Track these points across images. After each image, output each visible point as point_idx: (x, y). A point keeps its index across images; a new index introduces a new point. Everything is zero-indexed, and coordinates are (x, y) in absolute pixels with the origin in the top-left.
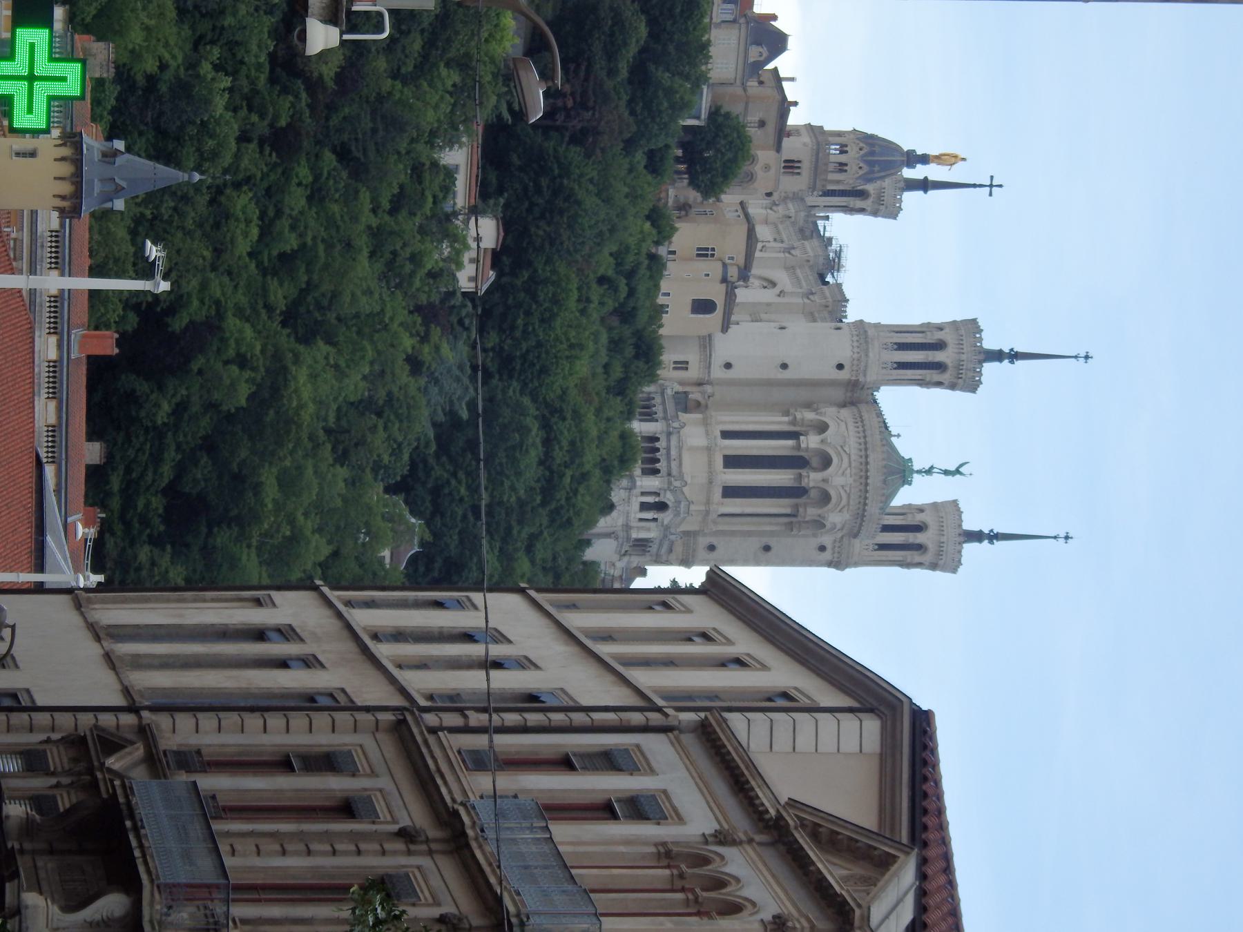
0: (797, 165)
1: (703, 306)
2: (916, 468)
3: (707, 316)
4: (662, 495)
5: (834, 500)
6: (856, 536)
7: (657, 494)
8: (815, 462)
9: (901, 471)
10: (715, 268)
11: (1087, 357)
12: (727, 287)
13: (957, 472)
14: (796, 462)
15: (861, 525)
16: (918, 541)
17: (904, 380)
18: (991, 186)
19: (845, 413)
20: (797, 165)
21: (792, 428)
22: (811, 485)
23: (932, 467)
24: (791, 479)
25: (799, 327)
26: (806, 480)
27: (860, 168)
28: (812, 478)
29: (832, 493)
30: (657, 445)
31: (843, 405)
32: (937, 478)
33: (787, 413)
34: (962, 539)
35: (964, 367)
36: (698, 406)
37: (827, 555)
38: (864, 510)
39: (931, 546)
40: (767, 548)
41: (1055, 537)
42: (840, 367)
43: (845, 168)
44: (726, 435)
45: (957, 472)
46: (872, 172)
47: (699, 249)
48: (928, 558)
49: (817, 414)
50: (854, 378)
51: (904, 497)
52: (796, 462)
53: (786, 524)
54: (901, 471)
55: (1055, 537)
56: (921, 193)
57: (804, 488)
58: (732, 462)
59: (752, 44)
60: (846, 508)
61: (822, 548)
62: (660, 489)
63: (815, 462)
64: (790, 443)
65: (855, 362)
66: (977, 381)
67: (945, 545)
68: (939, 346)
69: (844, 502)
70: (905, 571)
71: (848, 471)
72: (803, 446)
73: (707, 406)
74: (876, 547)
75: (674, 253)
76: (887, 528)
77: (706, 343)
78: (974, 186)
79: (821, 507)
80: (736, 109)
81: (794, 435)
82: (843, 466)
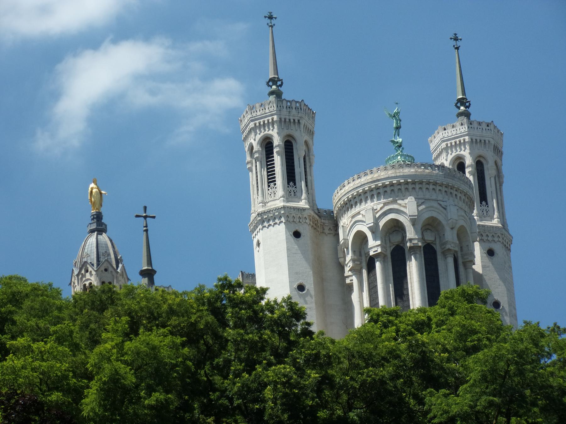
5: (435, 214)
26: (416, 242)
27: (106, 270)
29: (426, 216)
35: (287, 117)
37: (497, 248)
41: (457, 48)
42: (297, 235)
50: (308, 221)
55: (457, 48)
60: (441, 203)
63: (396, 239)
64: (378, 265)
66: (300, 105)
67: (474, 138)
68: (267, 144)
69: (435, 204)
70: (505, 180)
74: (484, 203)
79: (443, 227)
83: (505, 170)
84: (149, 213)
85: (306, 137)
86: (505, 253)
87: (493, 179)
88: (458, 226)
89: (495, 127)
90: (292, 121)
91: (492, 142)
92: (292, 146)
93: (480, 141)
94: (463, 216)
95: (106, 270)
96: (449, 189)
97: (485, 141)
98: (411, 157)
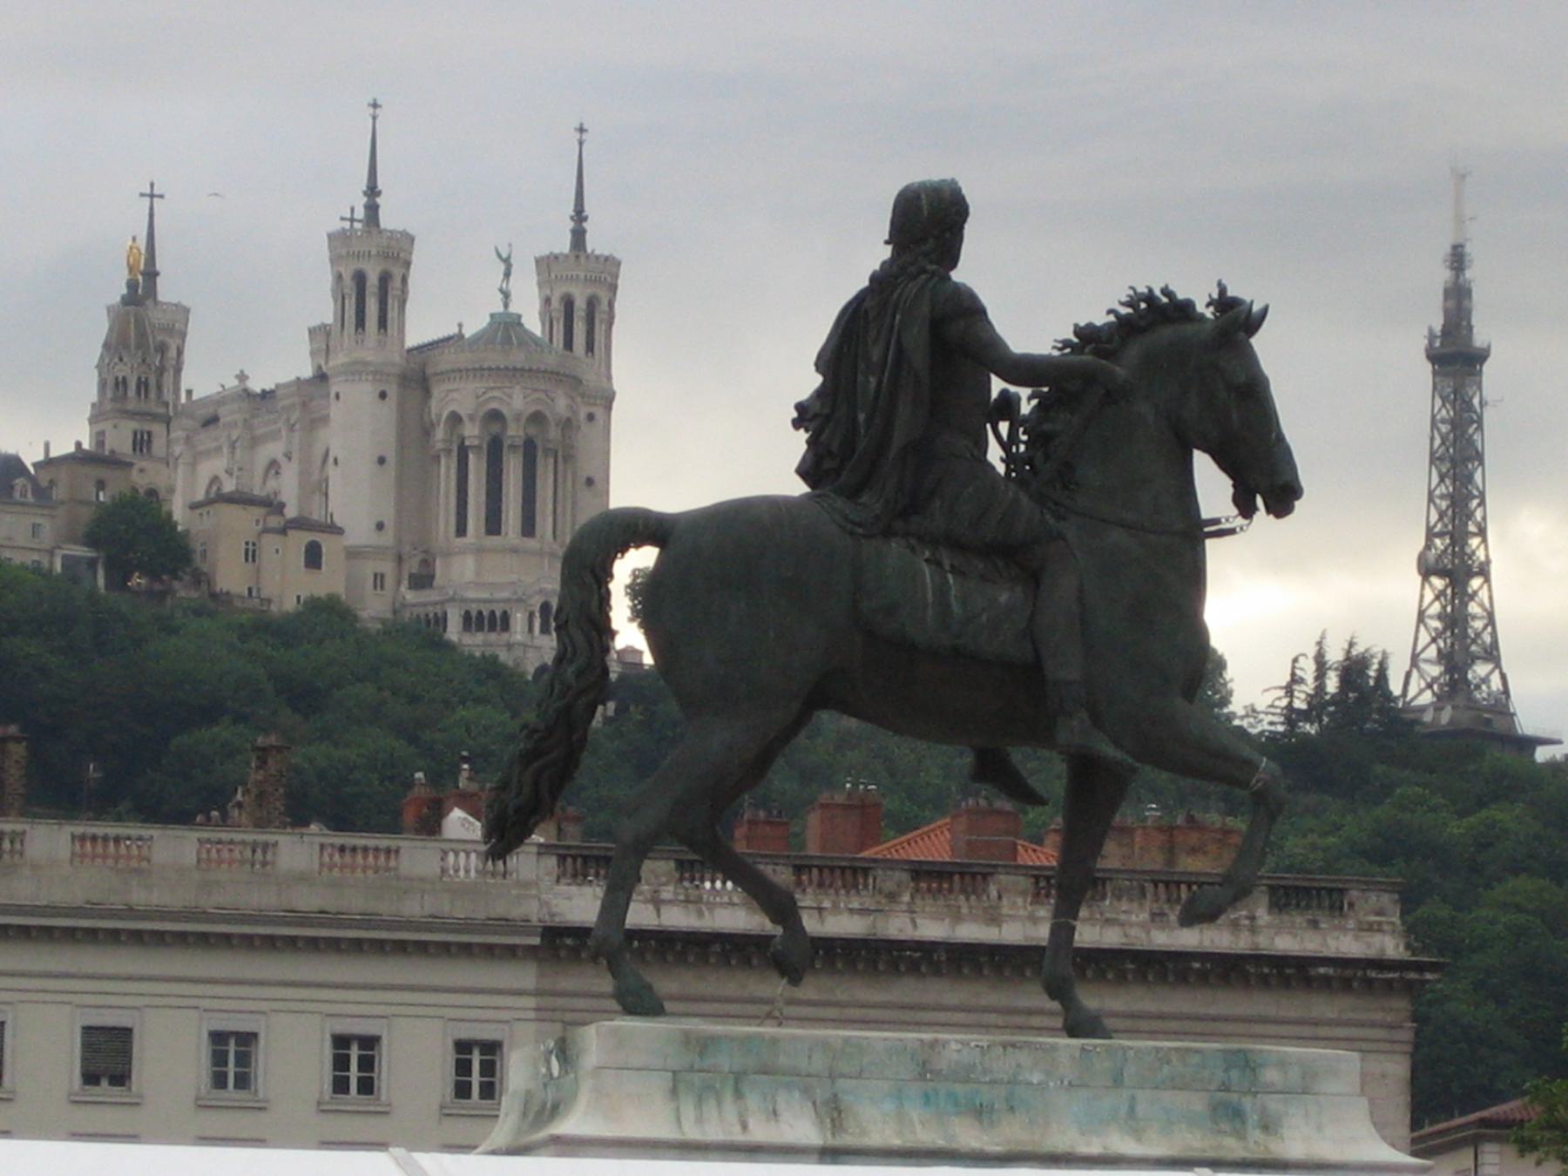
0: (139, 436)
1: (313, 557)
2: (501, 309)
3: (324, 550)
4: (531, 609)
5: (539, 408)
6: (580, 382)
7: (531, 615)
8: (495, 428)
9: (506, 327)
10: (270, 543)
12: (291, 528)
13: (507, 261)
15: (567, 376)
16: (584, 306)
18: (152, 196)
19: (438, 391)
20: (139, 436)
21: (455, 454)
22: (521, 433)
23: (501, 290)
25: (334, 438)
28: (514, 432)
29: (532, 409)
30: (474, 614)
31: (427, 392)
33: (437, 459)
36: (427, 563)
38: (552, 373)
39: (589, 291)
40: (590, 482)
42: (383, 395)
43: (143, 379)
44: (461, 530)
45: (507, 261)
47: (247, 560)
48: (604, 296)
49: (439, 425)
51: (533, 324)
54: (506, 327)
56: (159, 280)
57: (525, 443)
58: (493, 525)
59: (11, 496)
61: (591, 417)
62: (526, 610)
63: (495, 428)
65: (378, 377)
68: (360, 279)
70: (617, 320)
71: (506, 390)
72: (476, 442)
73: (425, 552)
75: (250, 590)
76: (569, 343)
77: (353, 554)
78: (151, 216)
80: (86, 514)
81: (463, 453)
91: (609, 279)
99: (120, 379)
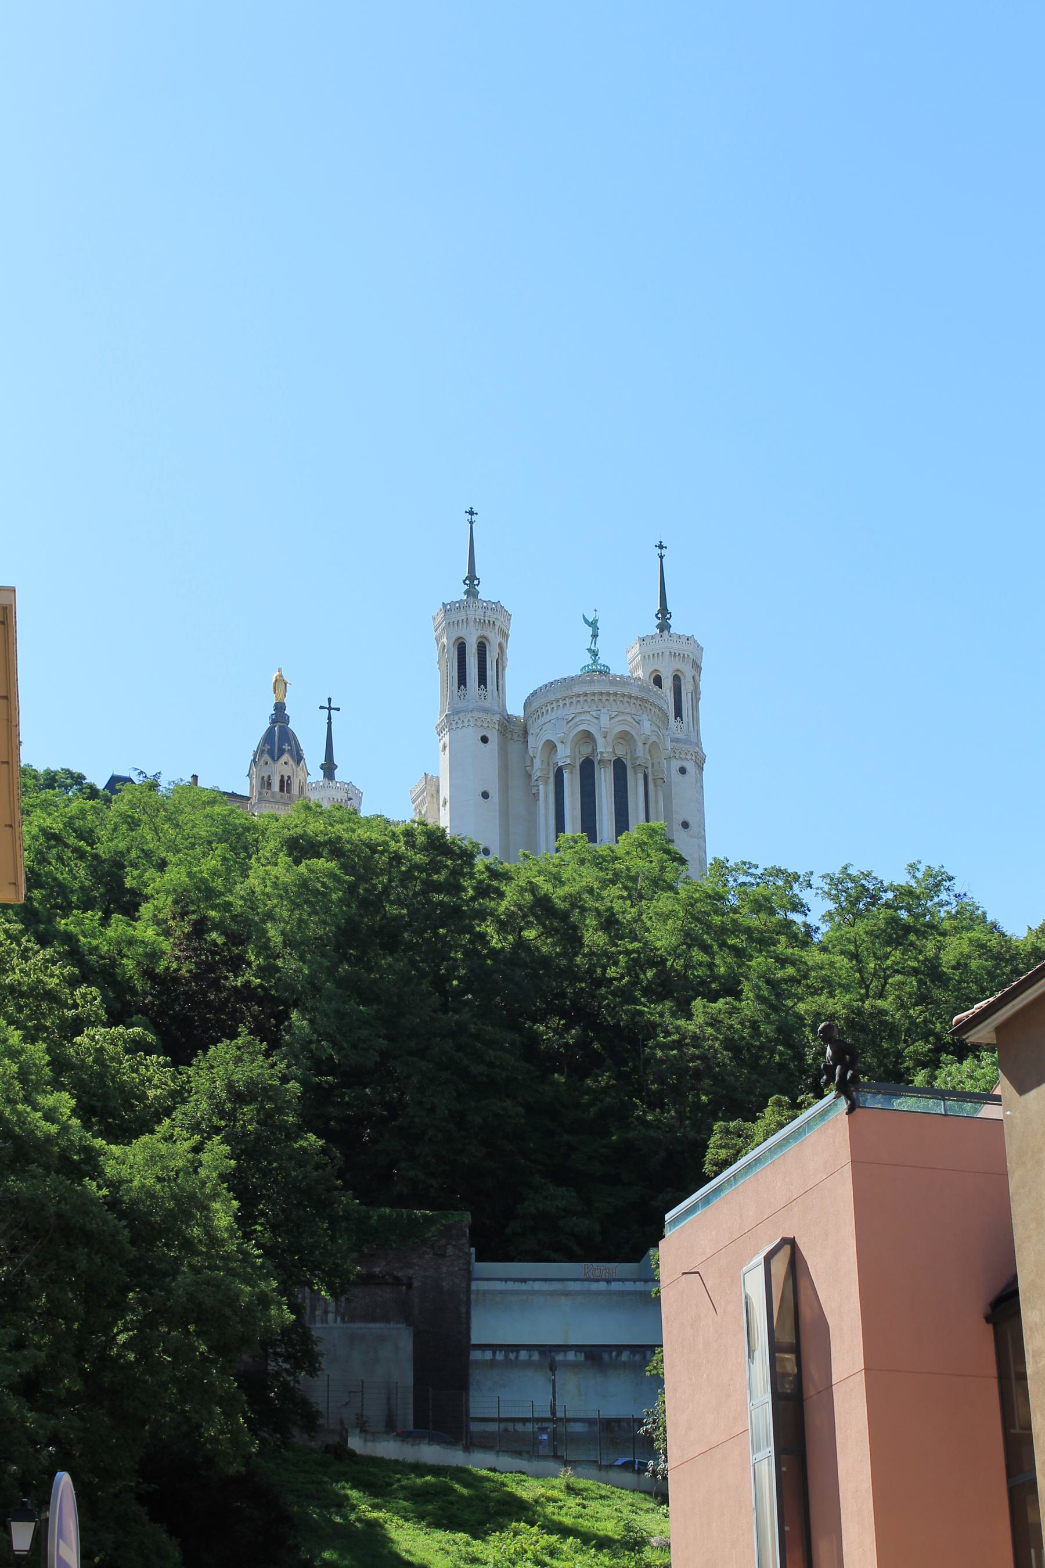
5: (627, 728)
11: (471, 513)
14: (587, 770)
17: (497, 682)
18: (330, 709)
21: (552, 780)
23: (589, 650)
24: (605, 773)
27: (286, 763)
32: (600, 644)
34: (666, 632)
37: (690, 766)
38: (637, 698)
40: (685, 825)
42: (485, 740)
43: (286, 778)
45: (593, 624)
46: (290, 752)
50: (497, 726)
52: (587, 770)
53: (656, 786)
55: (661, 557)
61: (683, 771)
63: (586, 751)
66: (496, 607)
69: (629, 718)
74: (678, 719)
78: (329, 724)
82: (588, 718)
83: (703, 686)
84: (332, 706)
85: (500, 639)
86: (697, 772)
87: (690, 695)
88: (650, 742)
89: (695, 641)
90: (487, 622)
91: (691, 657)
92: (485, 648)
93: (679, 654)
94: (657, 732)
95: (286, 763)
96: (643, 702)
97: (684, 655)
98: (607, 667)
99: (266, 779)
